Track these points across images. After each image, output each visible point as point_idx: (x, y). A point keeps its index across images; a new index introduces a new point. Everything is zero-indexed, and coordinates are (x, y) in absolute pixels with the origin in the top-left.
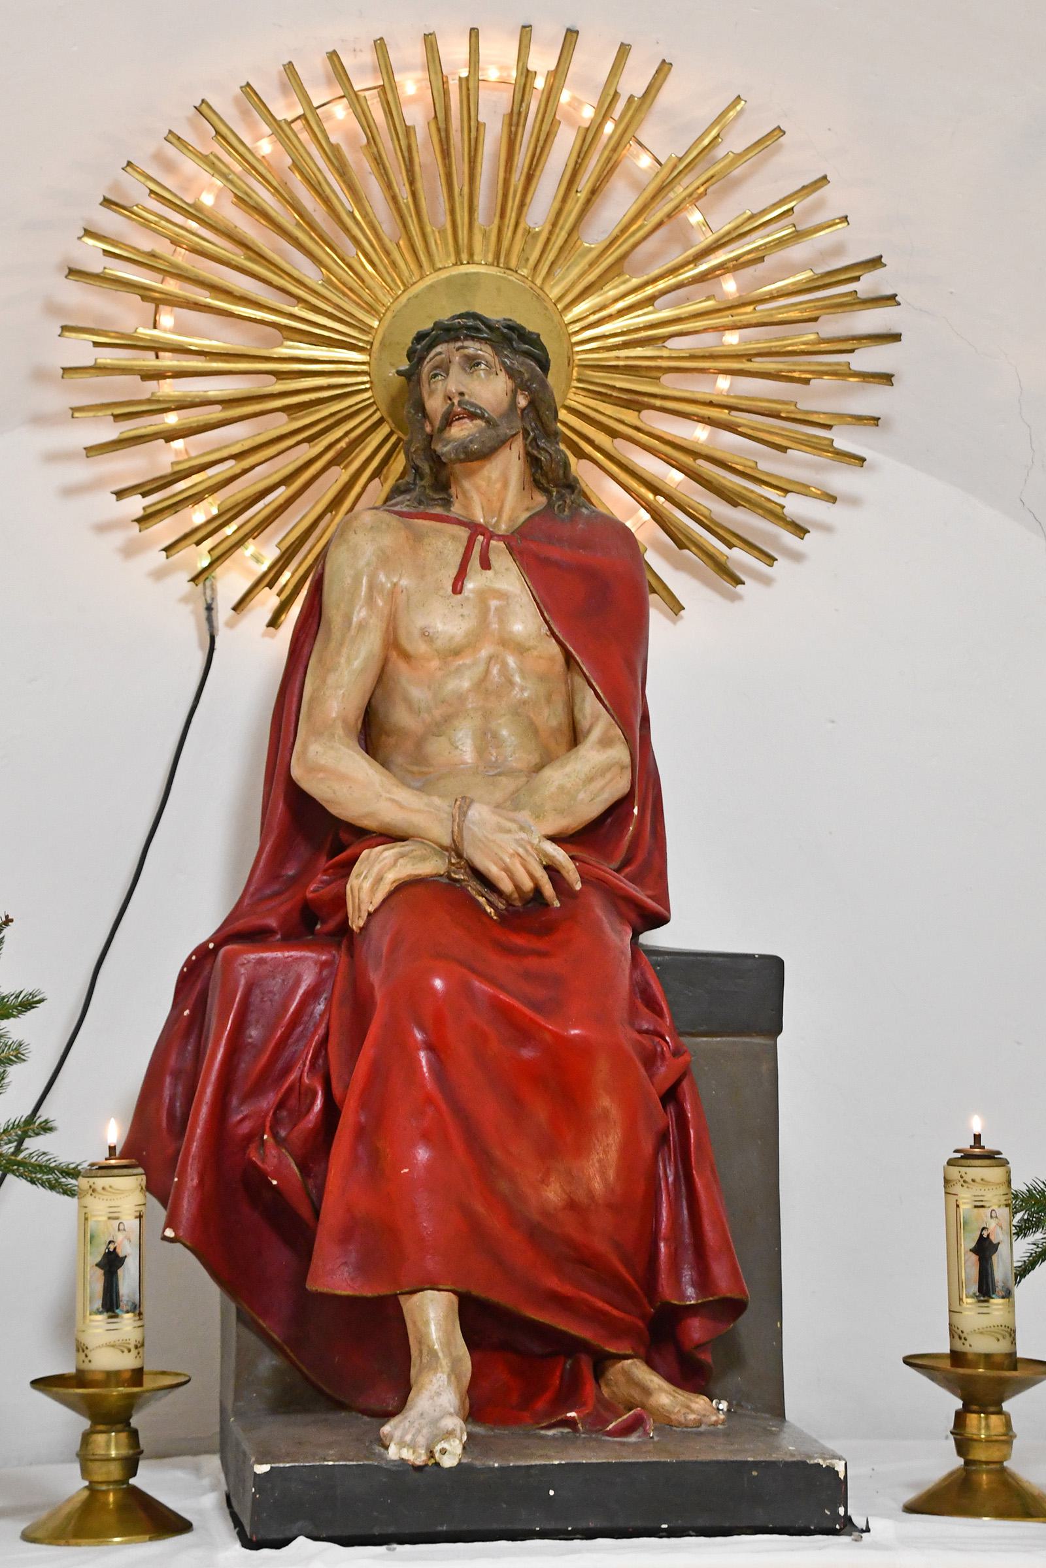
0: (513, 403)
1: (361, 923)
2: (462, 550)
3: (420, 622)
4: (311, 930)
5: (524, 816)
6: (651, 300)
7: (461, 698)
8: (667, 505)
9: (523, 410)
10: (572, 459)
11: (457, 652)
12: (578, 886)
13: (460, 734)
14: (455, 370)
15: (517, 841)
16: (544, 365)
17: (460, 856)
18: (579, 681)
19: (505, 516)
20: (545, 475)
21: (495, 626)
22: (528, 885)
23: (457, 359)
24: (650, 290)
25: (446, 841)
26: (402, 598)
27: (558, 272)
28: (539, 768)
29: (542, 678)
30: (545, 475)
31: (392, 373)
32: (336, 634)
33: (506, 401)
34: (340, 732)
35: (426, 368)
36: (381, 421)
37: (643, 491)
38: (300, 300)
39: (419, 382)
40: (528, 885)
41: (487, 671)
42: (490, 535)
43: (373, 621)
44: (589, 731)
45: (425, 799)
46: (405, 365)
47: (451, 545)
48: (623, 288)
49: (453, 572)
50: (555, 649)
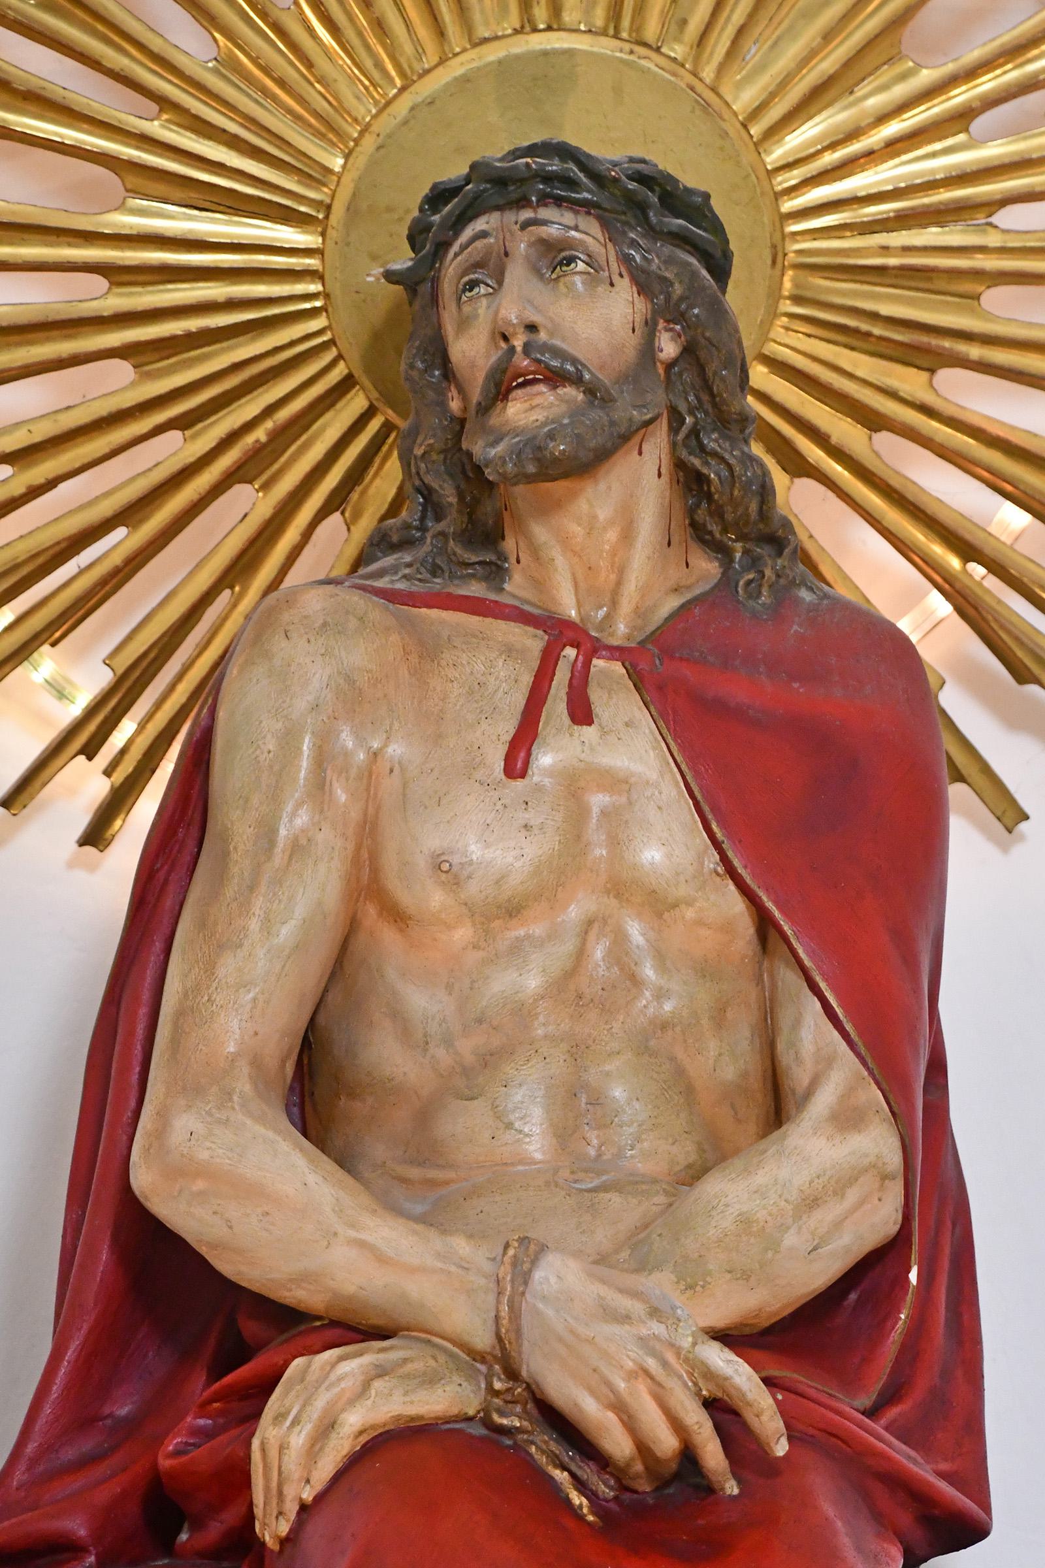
0: (648, 350)
1: (284, 1528)
2: (527, 679)
3: (432, 840)
4: (167, 1546)
5: (661, 1283)
6: (962, 118)
7: (522, 1012)
8: (993, 584)
9: (669, 366)
10: (779, 477)
11: (513, 910)
12: (781, 1448)
13: (518, 1095)
14: (516, 273)
15: (642, 1341)
16: (720, 268)
17: (512, 1374)
18: (789, 978)
19: (626, 606)
20: (718, 513)
21: (601, 852)
22: (667, 1443)
23: (521, 246)
24: (960, 96)
25: (483, 1340)
26: (389, 786)
27: (753, 52)
28: (694, 1175)
29: (705, 970)
30: (718, 513)
31: (373, 274)
32: (240, 865)
33: (631, 343)
34: (243, 1085)
35: (452, 268)
36: (346, 384)
37: (938, 550)
38: (164, 103)
39: (435, 299)
40: (667, 1443)
41: (581, 954)
42: (591, 648)
43: (325, 837)
44: (809, 1094)
45: (437, 1242)
46: (403, 260)
47: (502, 668)
48: (900, 91)
49: (507, 728)
50: (736, 905)
